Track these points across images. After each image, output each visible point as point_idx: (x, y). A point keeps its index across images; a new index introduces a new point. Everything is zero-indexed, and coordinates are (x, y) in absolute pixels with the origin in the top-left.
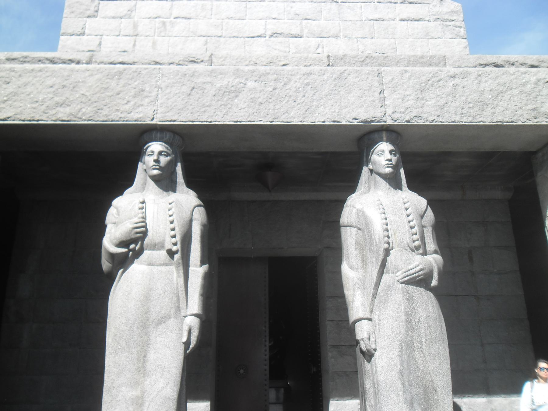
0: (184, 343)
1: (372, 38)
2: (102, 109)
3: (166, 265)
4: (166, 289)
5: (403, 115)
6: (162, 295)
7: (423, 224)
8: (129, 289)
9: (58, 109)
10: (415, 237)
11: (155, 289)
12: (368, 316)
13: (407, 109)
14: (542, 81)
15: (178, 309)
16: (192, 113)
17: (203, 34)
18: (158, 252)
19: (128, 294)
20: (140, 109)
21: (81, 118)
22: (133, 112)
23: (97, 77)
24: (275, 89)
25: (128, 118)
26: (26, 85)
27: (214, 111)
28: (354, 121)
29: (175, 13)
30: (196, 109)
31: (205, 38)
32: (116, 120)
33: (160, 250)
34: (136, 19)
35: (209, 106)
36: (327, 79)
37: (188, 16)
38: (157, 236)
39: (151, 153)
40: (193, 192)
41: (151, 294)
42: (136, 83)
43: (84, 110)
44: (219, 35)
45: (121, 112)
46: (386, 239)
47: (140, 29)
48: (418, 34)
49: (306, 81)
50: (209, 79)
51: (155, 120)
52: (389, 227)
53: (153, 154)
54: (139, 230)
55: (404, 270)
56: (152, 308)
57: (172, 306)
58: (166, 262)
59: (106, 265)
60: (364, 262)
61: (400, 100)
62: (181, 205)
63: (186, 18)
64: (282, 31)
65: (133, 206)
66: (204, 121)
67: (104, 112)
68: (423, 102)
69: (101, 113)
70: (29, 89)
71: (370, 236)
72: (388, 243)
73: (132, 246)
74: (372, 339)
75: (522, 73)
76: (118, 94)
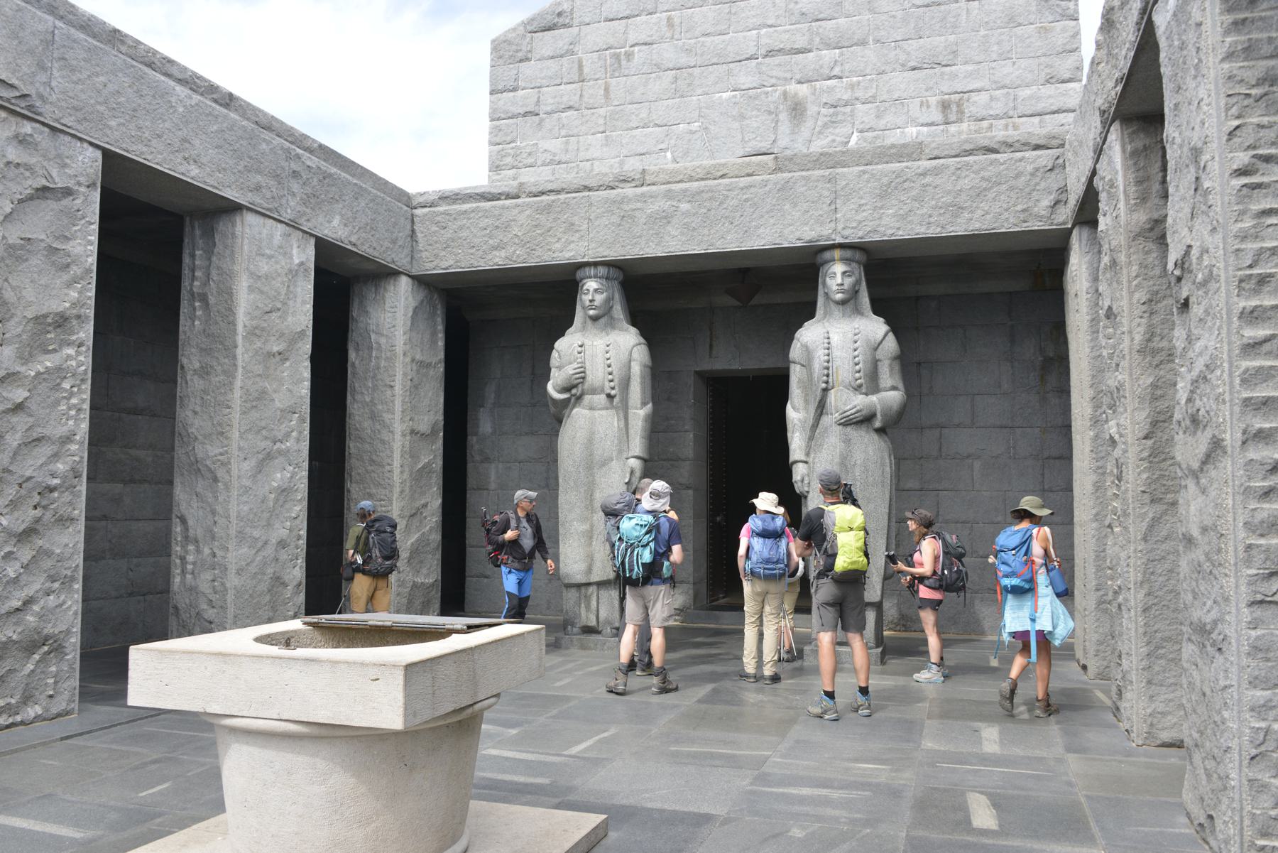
0: (626, 483)
1: (921, 38)
2: (534, 250)
5: (855, 231)
7: (877, 358)
9: (494, 253)
10: (858, 375)
12: (803, 458)
13: (860, 222)
14: (1042, 170)
15: (620, 451)
17: (671, 66)
18: (598, 396)
20: (572, 246)
21: (515, 261)
23: (528, 212)
24: (709, 210)
26: (461, 228)
28: (798, 241)
29: (632, 38)
31: (674, 72)
34: (580, 55)
35: (640, 237)
36: (770, 192)
37: (649, 40)
42: (565, 217)
43: (518, 252)
44: (692, 64)
46: (825, 378)
47: (586, 70)
48: (995, 22)
49: (745, 197)
50: (639, 205)
52: (830, 364)
54: (578, 376)
55: (841, 412)
59: (552, 409)
60: (806, 401)
61: (853, 212)
63: (645, 44)
64: (781, 46)
67: (537, 253)
68: (882, 211)
70: (464, 234)
71: (811, 374)
72: (827, 382)
73: (574, 391)
74: (806, 482)
75: (1016, 161)
76: (549, 231)
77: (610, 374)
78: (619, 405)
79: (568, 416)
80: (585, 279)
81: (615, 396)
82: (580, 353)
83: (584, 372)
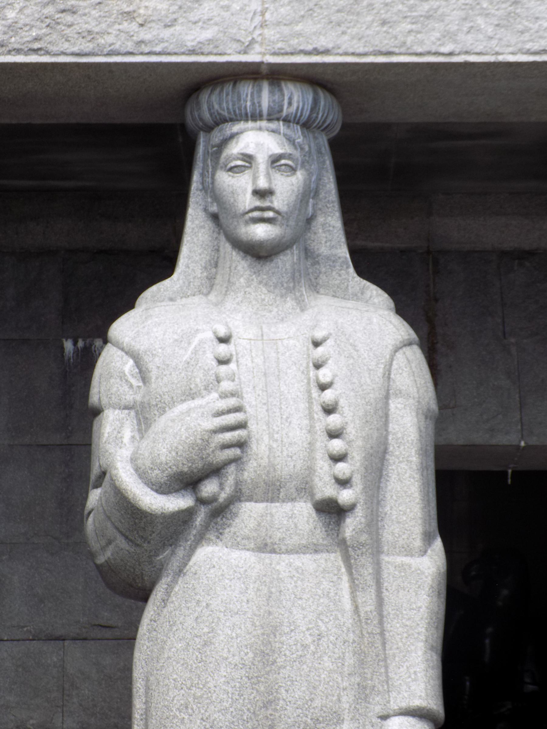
3: (316, 551)
4: (323, 628)
6: (312, 648)
8: (206, 630)
11: (287, 630)
16: (384, 23)
18: (288, 507)
19: (205, 644)
22: (181, 20)
25: (166, 44)
27: (462, 14)
30: (400, 7)
32: (123, 50)
33: (293, 500)
38: (285, 454)
39: (239, 163)
40: (380, 291)
41: (277, 645)
45: (140, 20)
51: (257, 48)
53: (247, 164)
56: (283, 691)
57: (345, 684)
58: (315, 541)
62: (354, 346)
65: (195, 352)
66: (429, 53)
69: (70, 26)
77: (333, 435)
78: (364, 538)
79: (180, 572)
80: (225, 121)
81: (352, 508)
82: (223, 362)
83: (242, 426)
